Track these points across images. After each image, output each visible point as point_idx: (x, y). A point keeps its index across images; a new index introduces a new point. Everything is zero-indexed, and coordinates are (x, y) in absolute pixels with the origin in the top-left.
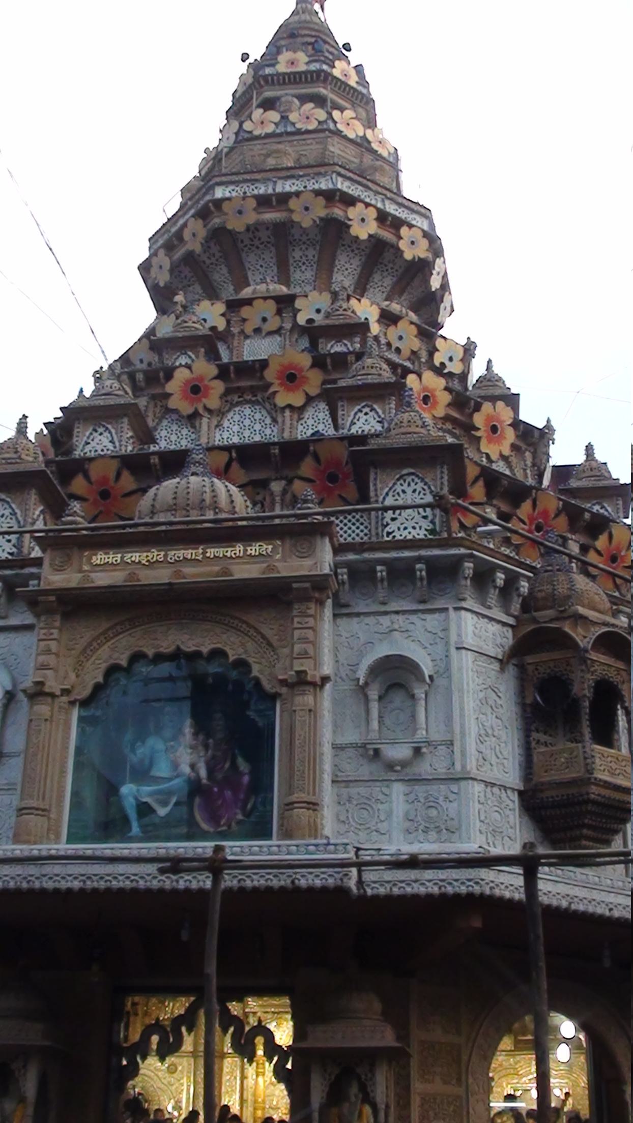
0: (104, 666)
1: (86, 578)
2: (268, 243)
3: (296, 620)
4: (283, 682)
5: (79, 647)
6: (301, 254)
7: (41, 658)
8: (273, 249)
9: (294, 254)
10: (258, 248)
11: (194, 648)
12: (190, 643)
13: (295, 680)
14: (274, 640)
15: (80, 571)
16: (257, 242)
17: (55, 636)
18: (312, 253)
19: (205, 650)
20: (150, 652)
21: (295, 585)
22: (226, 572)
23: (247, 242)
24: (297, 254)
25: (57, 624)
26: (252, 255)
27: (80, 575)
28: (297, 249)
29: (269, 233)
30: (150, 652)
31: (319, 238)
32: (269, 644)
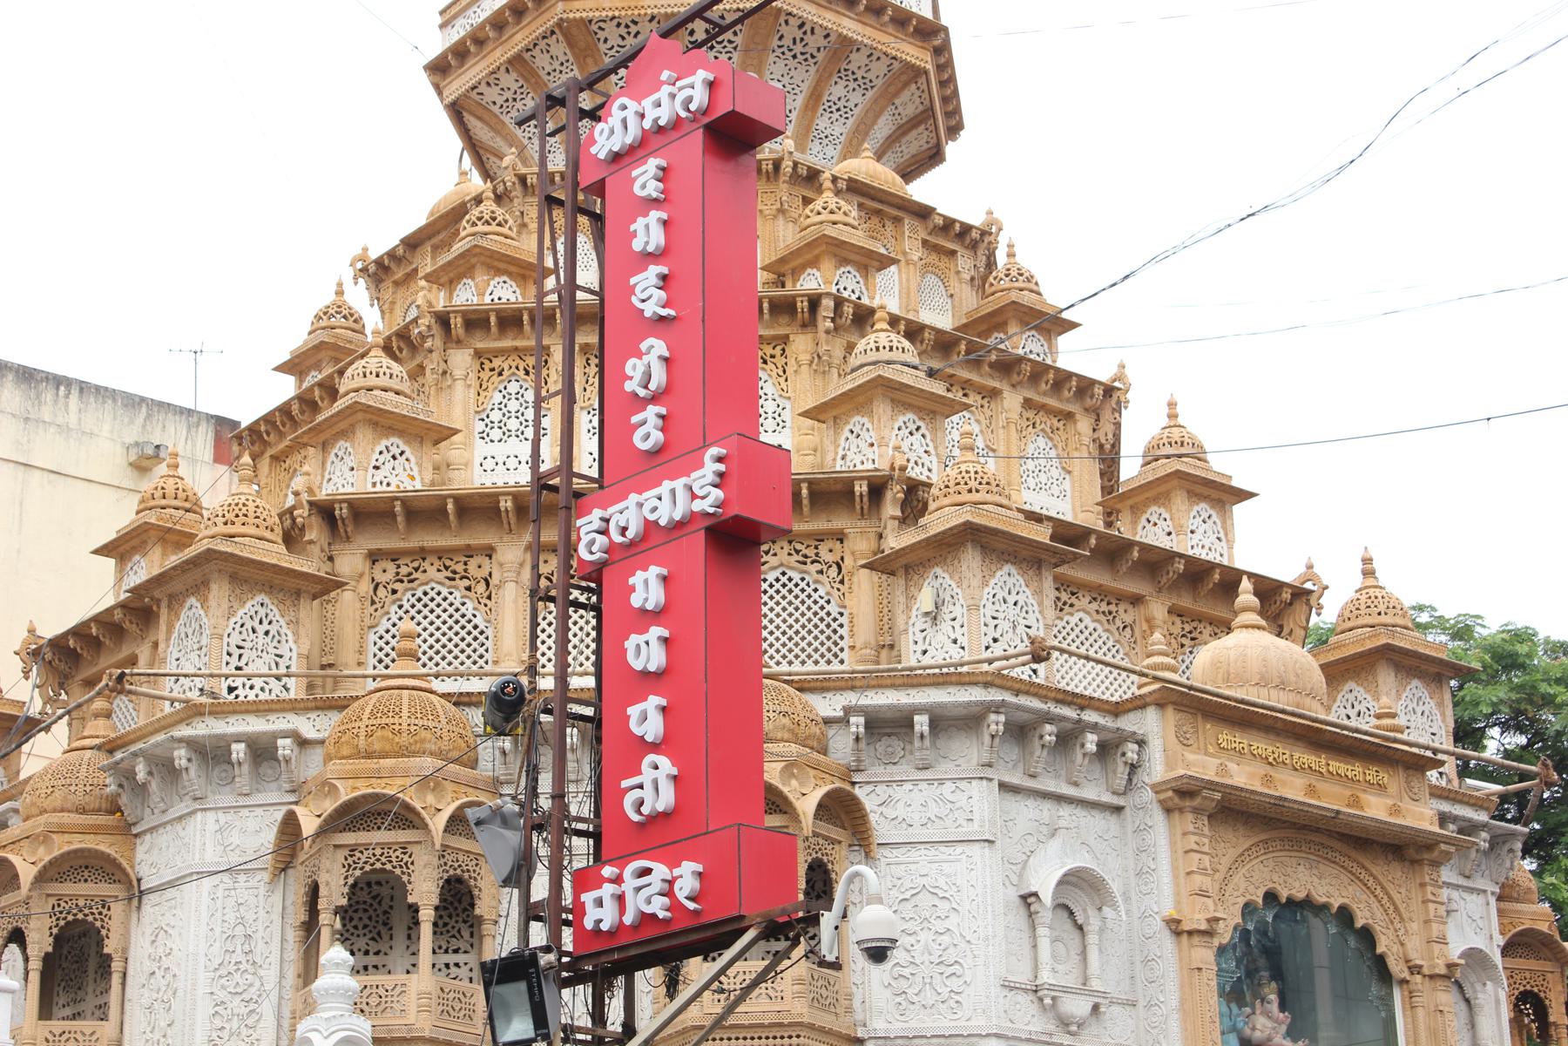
0: (1242, 901)
1: (1223, 770)
2: (813, 56)
3: (1429, 889)
4: (1415, 969)
5: (1223, 869)
6: (842, 93)
7: (1198, 879)
8: (813, 69)
9: (834, 89)
10: (794, 57)
11: (1323, 900)
12: (1321, 890)
13: (1443, 971)
14: (1402, 907)
15: (1206, 753)
16: (798, 48)
17: (1206, 849)
18: (856, 98)
19: (1336, 904)
20: (1284, 895)
21: (1443, 847)
22: (1355, 802)
23: (787, 42)
24: (837, 91)
25: (1206, 830)
26: (781, 63)
27: (1213, 763)
28: (842, 83)
29: (825, 43)
30: (1284, 895)
31: (879, 83)
32: (1396, 909)
